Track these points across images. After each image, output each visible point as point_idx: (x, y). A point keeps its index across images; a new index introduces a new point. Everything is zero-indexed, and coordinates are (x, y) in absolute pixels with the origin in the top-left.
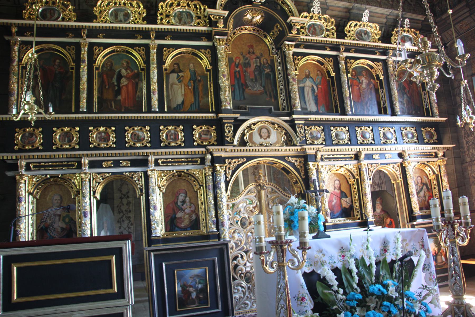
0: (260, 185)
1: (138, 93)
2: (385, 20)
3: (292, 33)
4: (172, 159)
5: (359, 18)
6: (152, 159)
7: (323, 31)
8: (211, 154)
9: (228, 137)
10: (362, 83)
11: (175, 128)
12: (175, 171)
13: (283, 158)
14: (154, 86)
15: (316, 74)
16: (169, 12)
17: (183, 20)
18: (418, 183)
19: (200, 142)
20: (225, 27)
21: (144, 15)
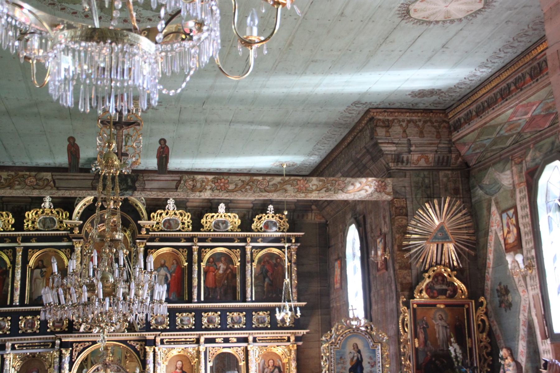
0: (106, 364)
1: (5, 288)
2: (251, 205)
3: (141, 234)
4: (27, 343)
5: (216, 211)
6: (9, 344)
7: (179, 225)
8: (60, 340)
9: (76, 325)
10: (219, 269)
11: (33, 318)
12: (28, 354)
13: (124, 342)
14: (18, 284)
15: (171, 262)
16: (35, 219)
17: (47, 225)
18: (269, 366)
19: (53, 329)
20: (80, 233)
21: (13, 221)
